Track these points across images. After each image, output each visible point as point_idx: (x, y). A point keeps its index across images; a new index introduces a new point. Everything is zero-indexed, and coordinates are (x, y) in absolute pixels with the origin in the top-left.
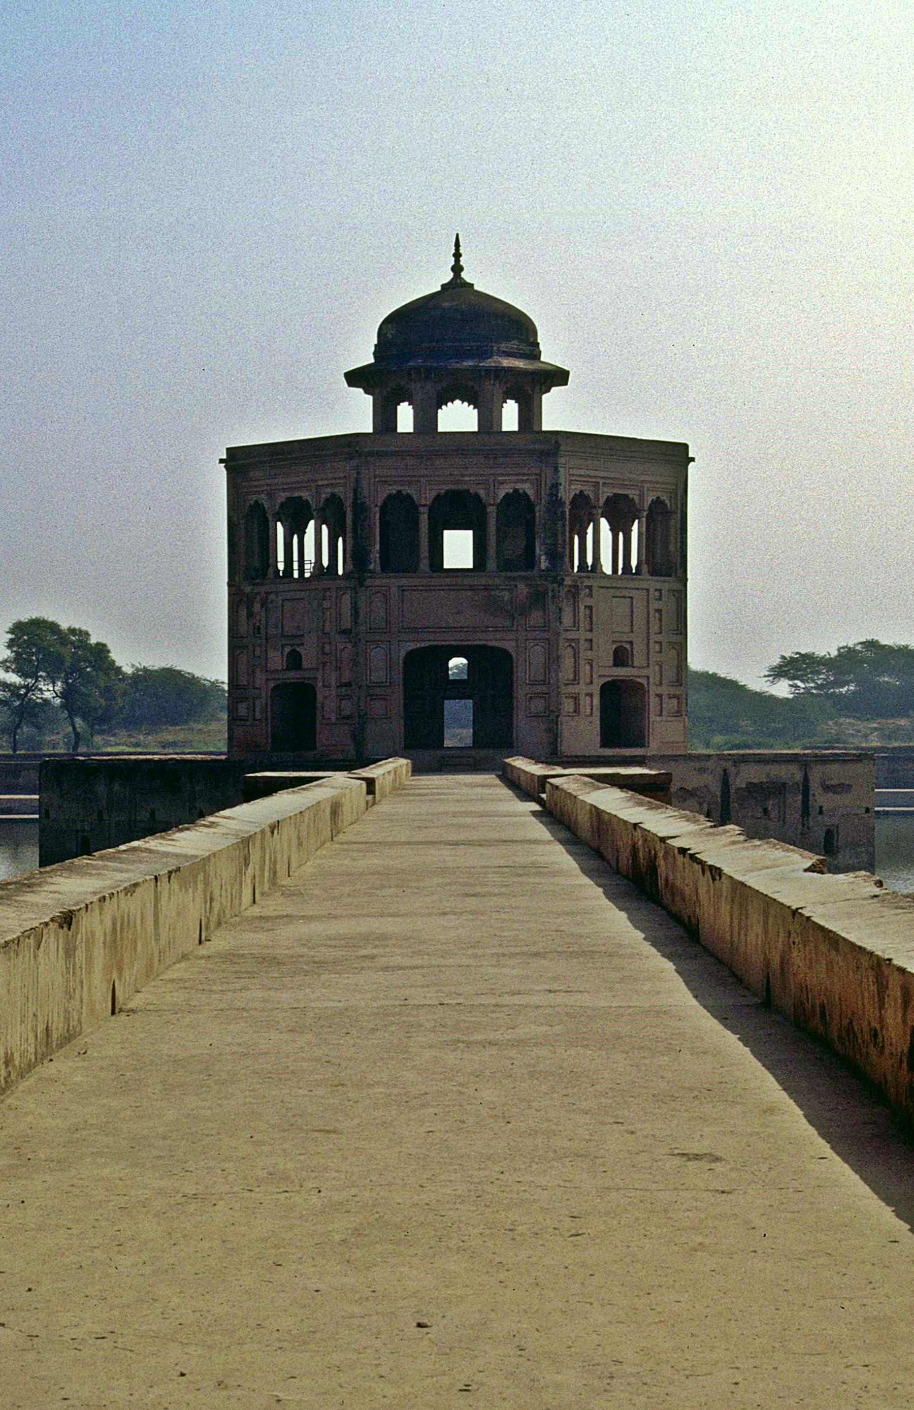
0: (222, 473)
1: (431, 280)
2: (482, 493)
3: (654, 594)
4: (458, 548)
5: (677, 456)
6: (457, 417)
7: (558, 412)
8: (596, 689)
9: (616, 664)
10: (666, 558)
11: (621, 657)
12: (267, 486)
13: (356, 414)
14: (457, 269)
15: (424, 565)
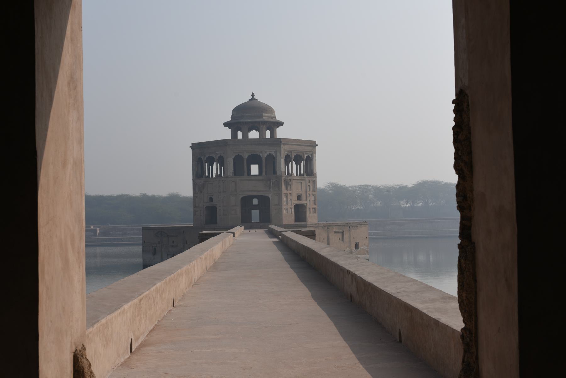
0: (190, 150)
1: (245, 99)
2: (261, 155)
3: (307, 181)
4: (255, 169)
5: (313, 144)
6: (254, 135)
7: (281, 133)
8: (293, 206)
9: (298, 200)
10: (310, 172)
11: (299, 197)
12: (203, 153)
13: (226, 134)
14: (253, 95)
15: (246, 173)
